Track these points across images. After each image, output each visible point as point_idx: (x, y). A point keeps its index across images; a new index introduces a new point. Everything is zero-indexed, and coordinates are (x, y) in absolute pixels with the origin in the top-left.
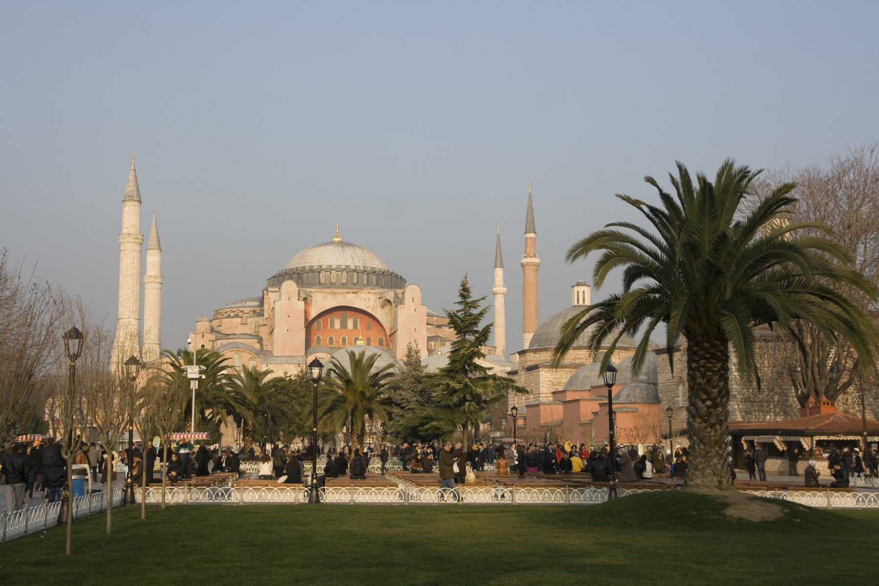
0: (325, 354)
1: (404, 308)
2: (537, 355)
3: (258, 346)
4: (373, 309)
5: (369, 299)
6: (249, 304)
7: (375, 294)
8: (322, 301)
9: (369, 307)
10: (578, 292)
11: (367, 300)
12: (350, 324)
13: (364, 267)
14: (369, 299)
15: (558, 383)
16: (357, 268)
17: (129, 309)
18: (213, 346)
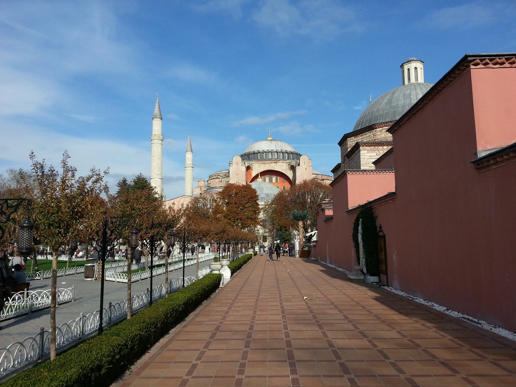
4: (285, 171)
5: (283, 166)
7: (286, 163)
9: (283, 170)
10: (409, 69)
13: (281, 150)
14: (283, 166)
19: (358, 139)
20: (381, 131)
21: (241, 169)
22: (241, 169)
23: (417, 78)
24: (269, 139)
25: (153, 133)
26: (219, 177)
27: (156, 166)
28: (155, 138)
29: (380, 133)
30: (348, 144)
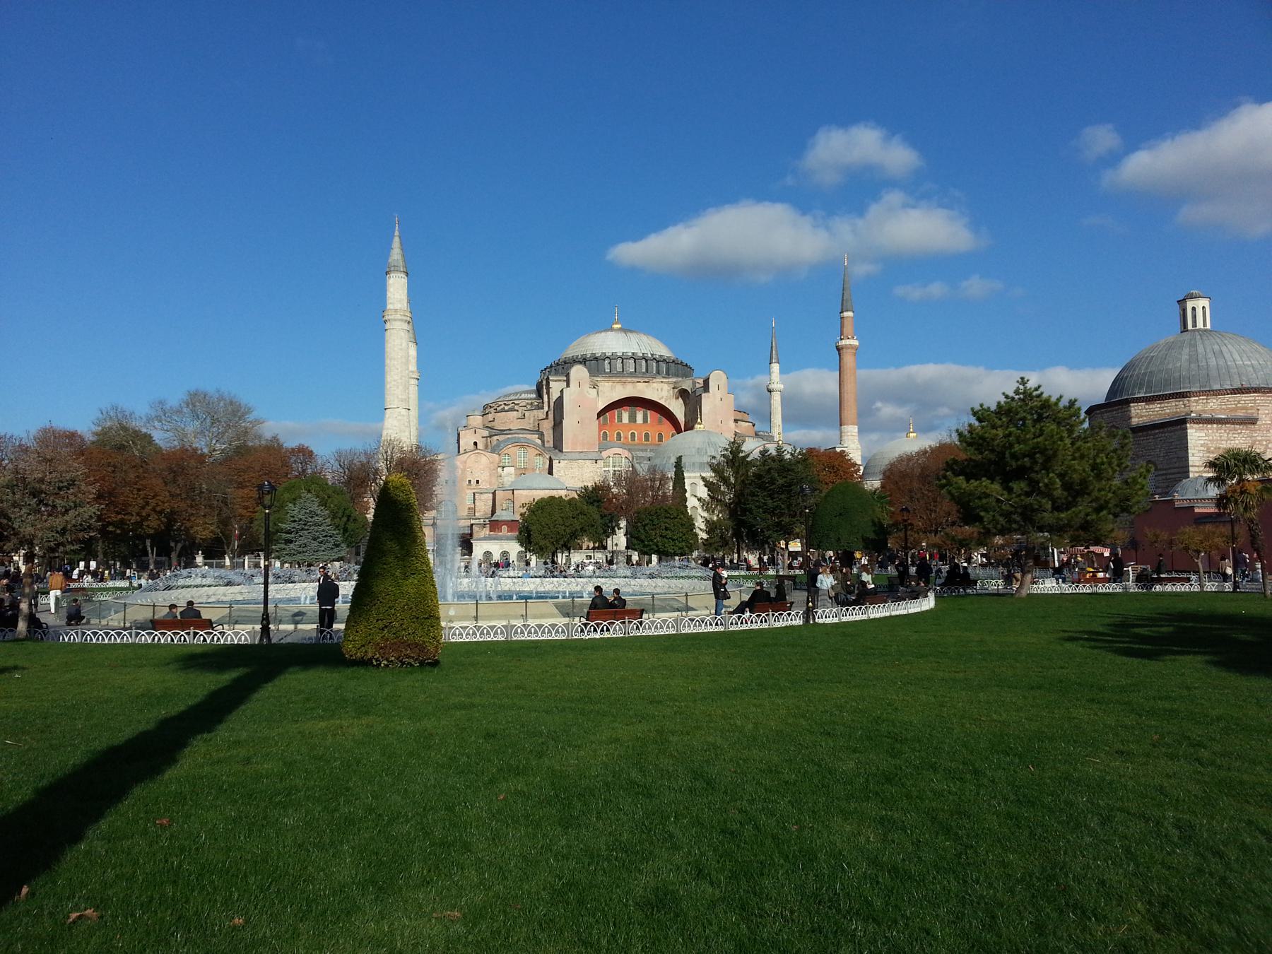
0: (621, 449)
1: (708, 397)
2: (1156, 406)
3: (539, 442)
5: (662, 390)
6: (523, 396)
7: (668, 383)
8: (613, 391)
9: (662, 397)
10: (1194, 309)
11: (660, 390)
12: (640, 416)
13: (652, 355)
14: (662, 390)
15: (1215, 448)
16: (645, 355)
17: (398, 397)
18: (487, 443)
19: (1154, 407)
20: (1197, 402)
21: (587, 394)
22: (587, 394)
23: (1205, 324)
24: (616, 326)
25: (389, 306)
26: (516, 407)
27: (400, 381)
28: (396, 318)
29: (1195, 404)
30: (1133, 411)
